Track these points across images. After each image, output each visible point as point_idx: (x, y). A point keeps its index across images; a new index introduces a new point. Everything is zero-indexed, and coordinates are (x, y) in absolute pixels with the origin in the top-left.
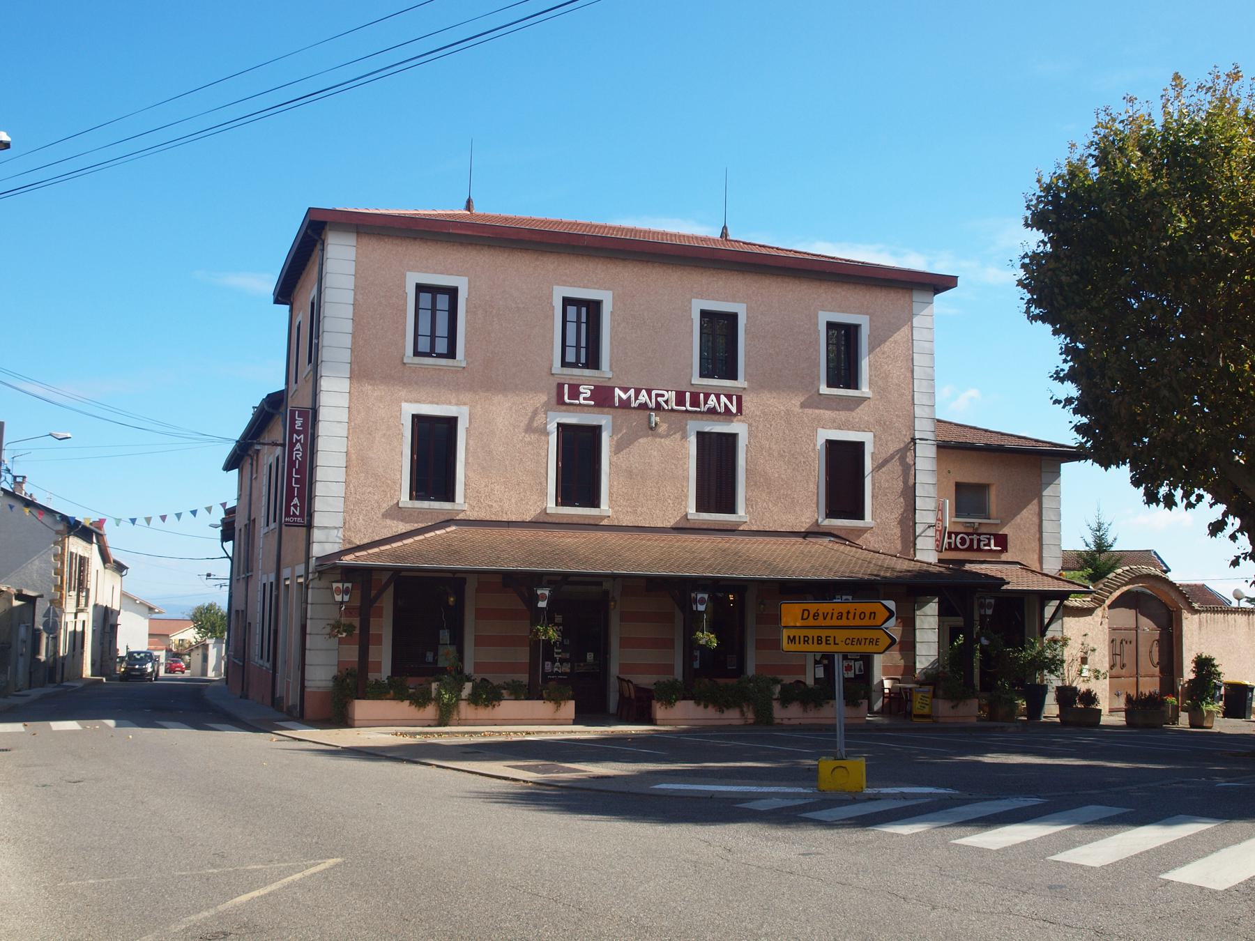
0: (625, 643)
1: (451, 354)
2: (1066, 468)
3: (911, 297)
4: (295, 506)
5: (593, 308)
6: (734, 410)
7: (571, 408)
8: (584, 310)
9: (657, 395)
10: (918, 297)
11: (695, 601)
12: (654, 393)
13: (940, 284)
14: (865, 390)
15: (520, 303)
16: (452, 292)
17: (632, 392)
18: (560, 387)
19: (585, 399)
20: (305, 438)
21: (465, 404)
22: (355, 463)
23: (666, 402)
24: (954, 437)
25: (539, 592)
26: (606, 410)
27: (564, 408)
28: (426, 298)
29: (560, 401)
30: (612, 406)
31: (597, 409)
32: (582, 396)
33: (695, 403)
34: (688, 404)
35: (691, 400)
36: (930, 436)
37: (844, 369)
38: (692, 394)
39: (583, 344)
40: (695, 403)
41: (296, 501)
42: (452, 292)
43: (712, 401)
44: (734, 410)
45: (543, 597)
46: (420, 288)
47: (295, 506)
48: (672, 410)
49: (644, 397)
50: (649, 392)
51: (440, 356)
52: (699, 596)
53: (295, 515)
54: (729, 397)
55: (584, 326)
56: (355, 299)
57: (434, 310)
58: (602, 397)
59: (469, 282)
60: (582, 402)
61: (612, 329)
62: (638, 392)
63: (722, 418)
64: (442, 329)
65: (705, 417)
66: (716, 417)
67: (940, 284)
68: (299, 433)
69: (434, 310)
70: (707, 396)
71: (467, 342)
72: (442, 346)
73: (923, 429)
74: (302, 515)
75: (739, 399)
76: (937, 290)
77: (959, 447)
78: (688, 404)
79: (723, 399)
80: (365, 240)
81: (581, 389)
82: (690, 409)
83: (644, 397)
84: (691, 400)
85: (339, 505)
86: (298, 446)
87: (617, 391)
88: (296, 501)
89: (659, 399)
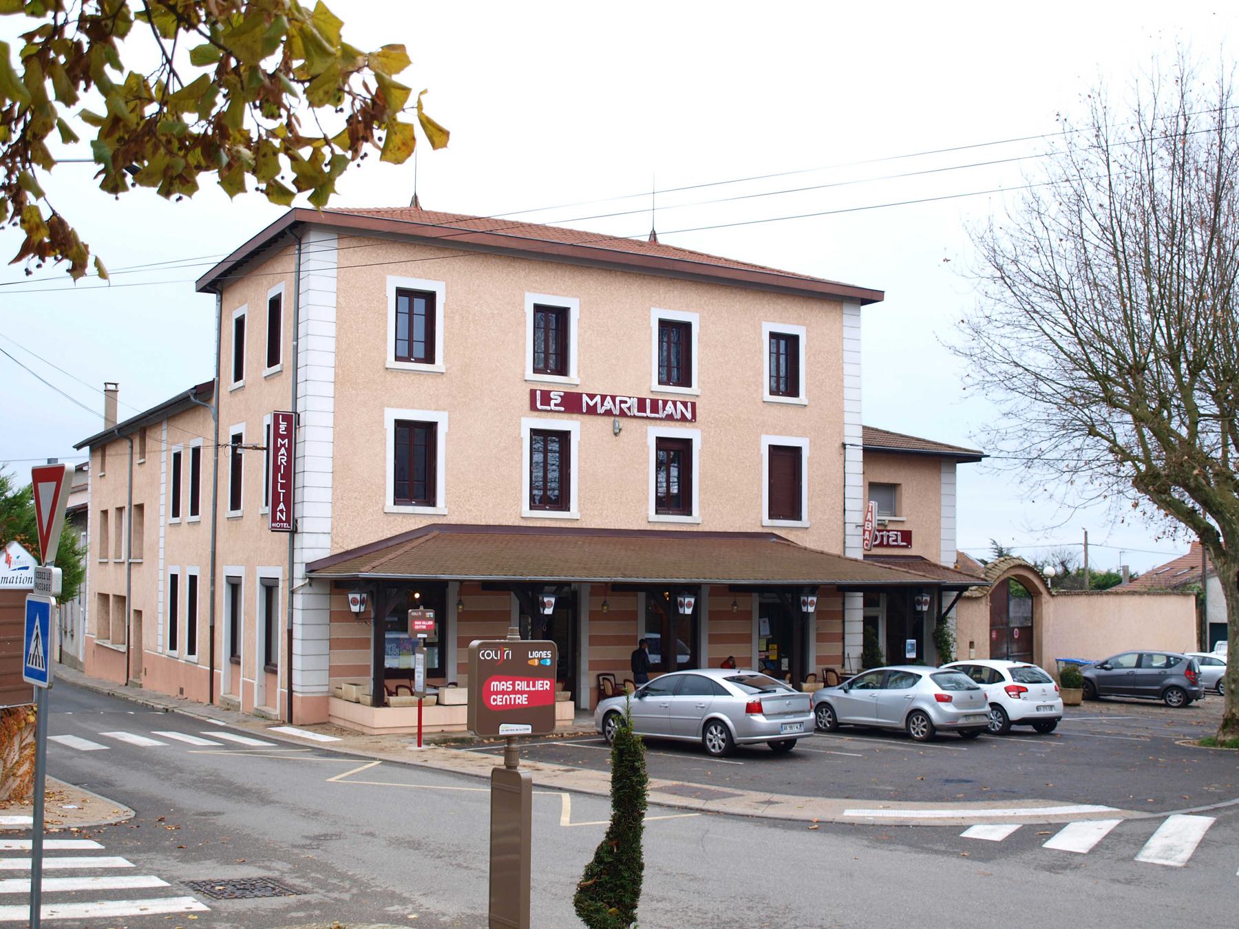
0: (594, 641)
1: (429, 358)
2: (960, 467)
3: (841, 309)
4: (281, 511)
5: (792, 341)
6: (689, 416)
7: (543, 414)
8: (782, 343)
9: (621, 402)
10: (848, 309)
11: (682, 605)
12: (618, 400)
13: (869, 297)
14: (803, 398)
15: (488, 313)
16: (430, 297)
17: (598, 399)
18: (533, 392)
19: (556, 405)
20: (290, 442)
21: (444, 410)
22: (340, 470)
23: (629, 408)
24: (878, 443)
25: (546, 600)
26: (575, 416)
27: (536, 413)
28: (405, 300)
29: (533, 407)
30: (580, 411)
31: (566, 416)
32: (553, 402)
33: (655, 409)
34: (648, 410)
35: (649, 408)
36: (860, 442)
37: (787, 381)
38: (652, 400)
39: (782, 373)
40: (655, 409)
41: (282, 506)
42: (430, 297)
43: (670, 408)
44: (689, 416)
45: (550, 603)
46: (401, 292)
47: (281, 511)
48: (635, 417)
49: (608, 404)
50: (613, 398)
51: (418, 361)
52: (687, 600)
53: (281, 521)
54: (685, 404)
55: (782, 359)
56: (338, 302)
57: (411, 314)
58: (572, 403)
59: (447, 287)
60: (553, 407)
61: (579, 335)
62: (603, 398)
63: (678, 424)
64: (419, 334)
65: (663, 423)
66: (672, 423)
67: (869, 297)
68: (283, 437)
69: (411, 314)
70: (665, 403)
71: (446, 347)
72: (419, 350)
73: (854, 437)
74: (288, 520)
75: (693, 405)
76: (865, 302)
77: (885, 452)
78: (648, 410)
79: (679, 406)
80: (346, 242)
81: (552, 395)
82: (637, 414)
83: (608, 404)
84: (649, 408)
85: (327, 510)
86: (283, 451)
87: (585, 398)
88: (282, 506)
89: (623, 406)
